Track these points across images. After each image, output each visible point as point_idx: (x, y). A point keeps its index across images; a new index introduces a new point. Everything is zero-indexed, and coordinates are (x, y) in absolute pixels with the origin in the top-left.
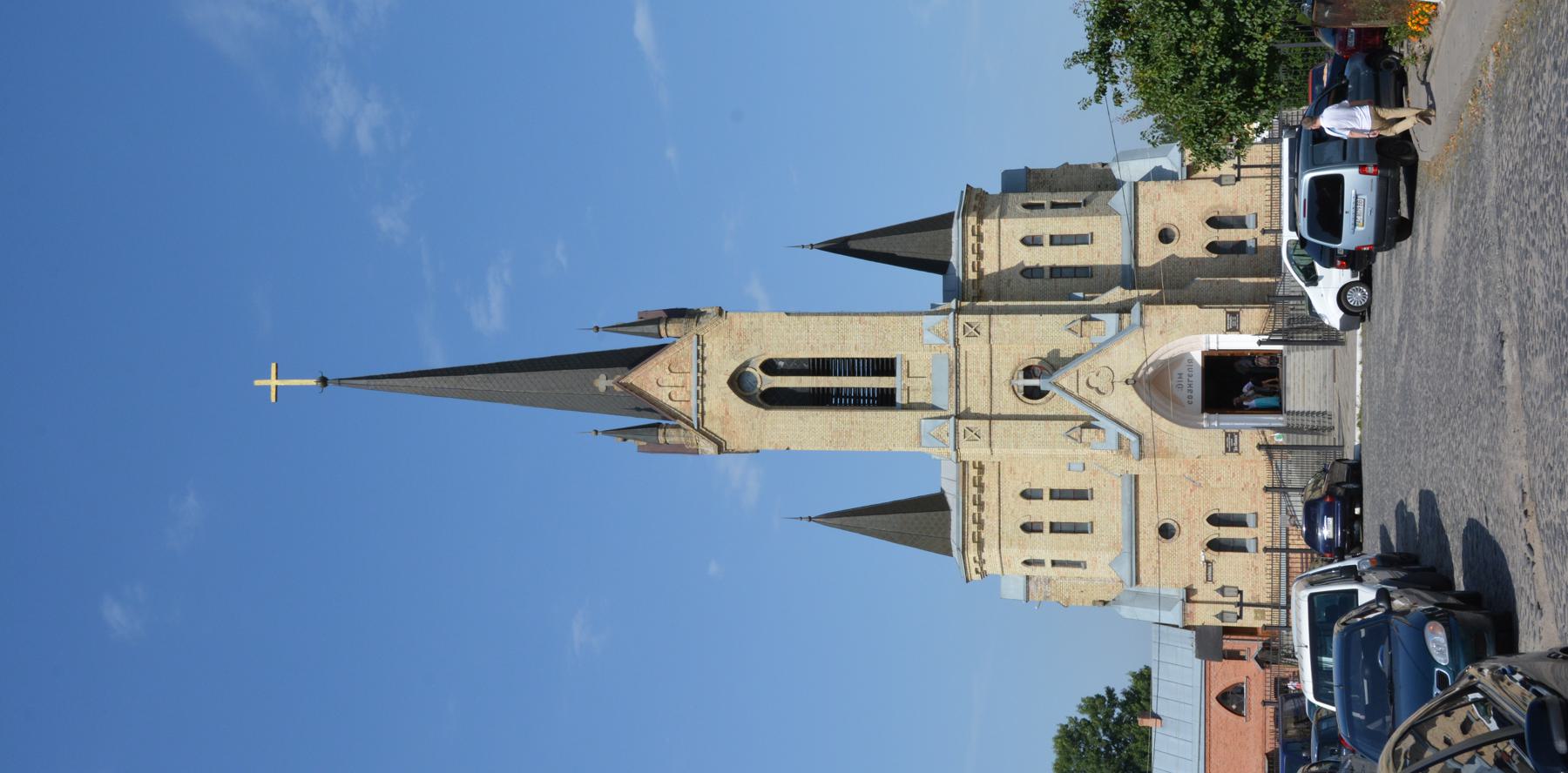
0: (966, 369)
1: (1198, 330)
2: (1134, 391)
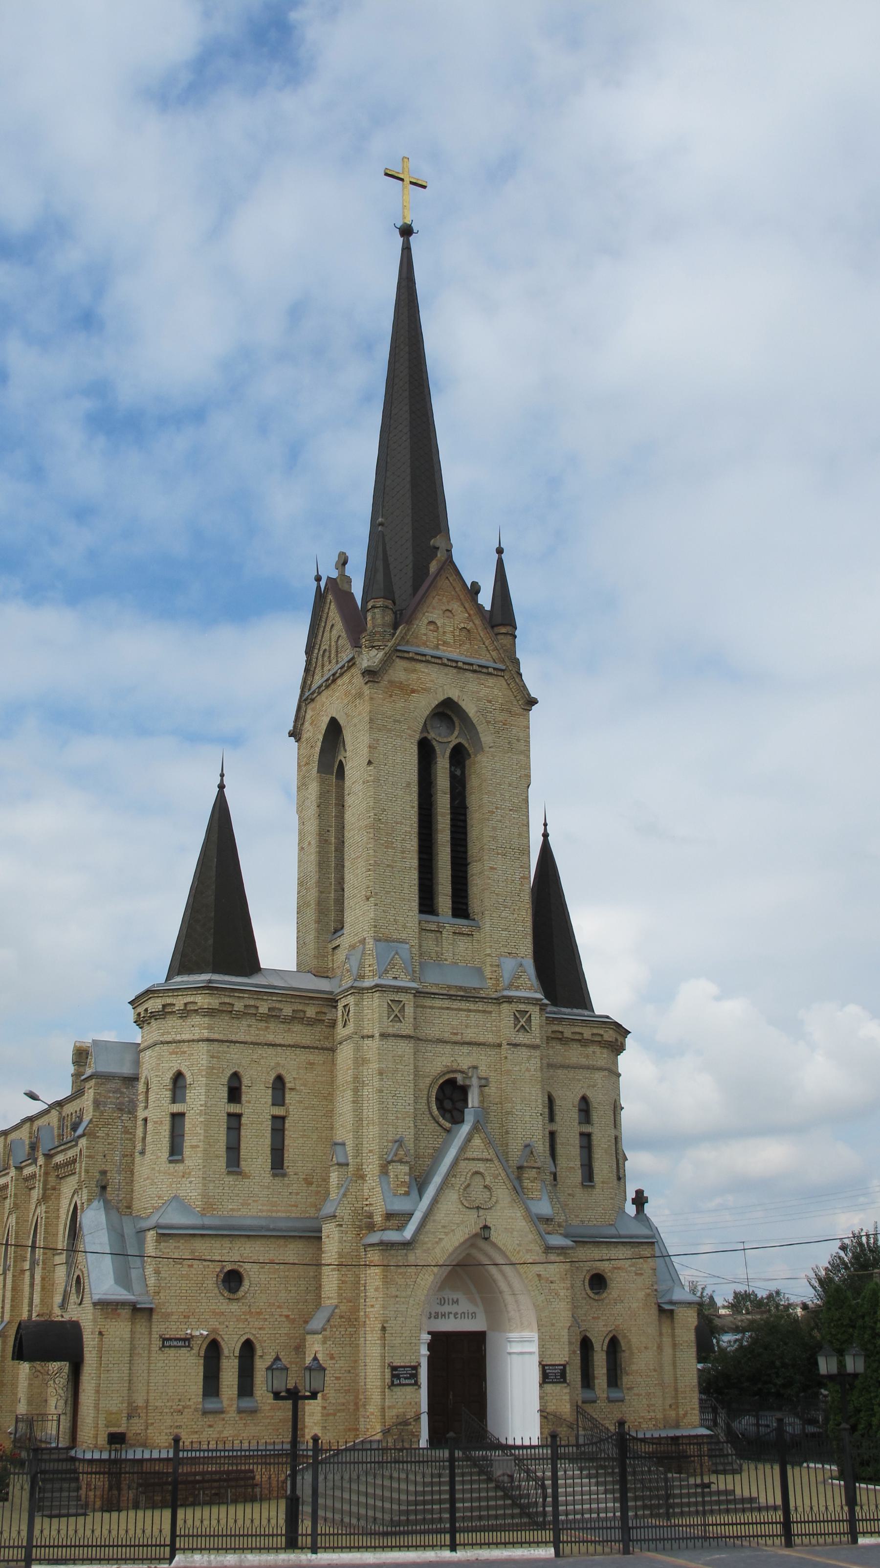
0: (470, 1011)
1: (542, 1325)
2: (467, 1236)
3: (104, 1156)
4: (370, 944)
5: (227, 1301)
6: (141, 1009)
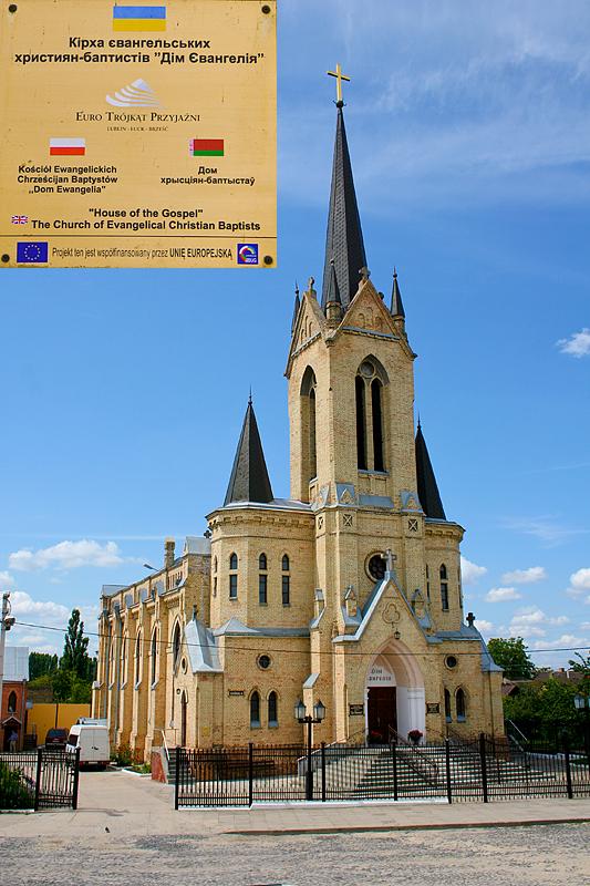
4: (334, 485)
6: (212, 521)
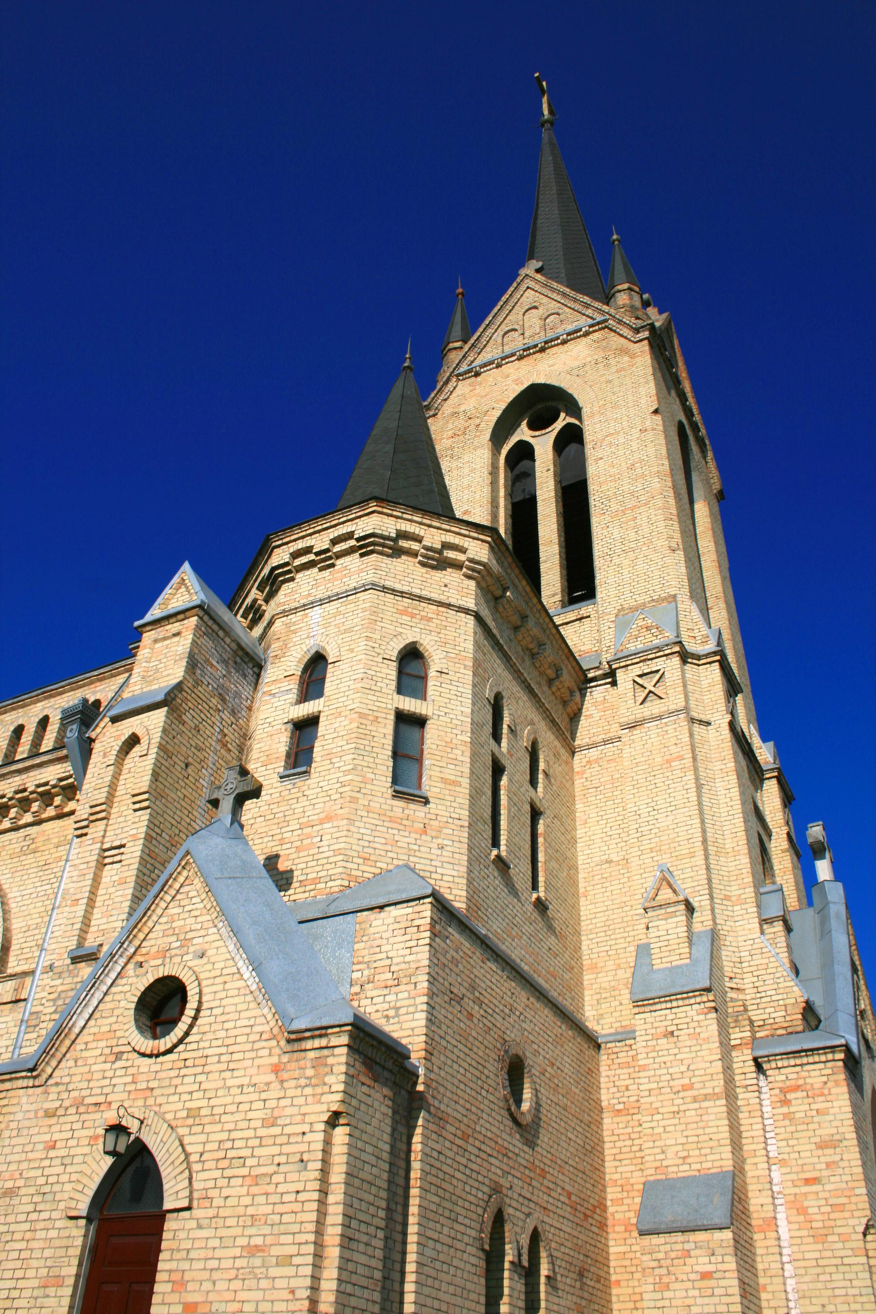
3: (187, 765)
5: (510, 1123)
